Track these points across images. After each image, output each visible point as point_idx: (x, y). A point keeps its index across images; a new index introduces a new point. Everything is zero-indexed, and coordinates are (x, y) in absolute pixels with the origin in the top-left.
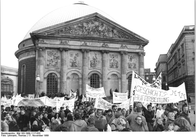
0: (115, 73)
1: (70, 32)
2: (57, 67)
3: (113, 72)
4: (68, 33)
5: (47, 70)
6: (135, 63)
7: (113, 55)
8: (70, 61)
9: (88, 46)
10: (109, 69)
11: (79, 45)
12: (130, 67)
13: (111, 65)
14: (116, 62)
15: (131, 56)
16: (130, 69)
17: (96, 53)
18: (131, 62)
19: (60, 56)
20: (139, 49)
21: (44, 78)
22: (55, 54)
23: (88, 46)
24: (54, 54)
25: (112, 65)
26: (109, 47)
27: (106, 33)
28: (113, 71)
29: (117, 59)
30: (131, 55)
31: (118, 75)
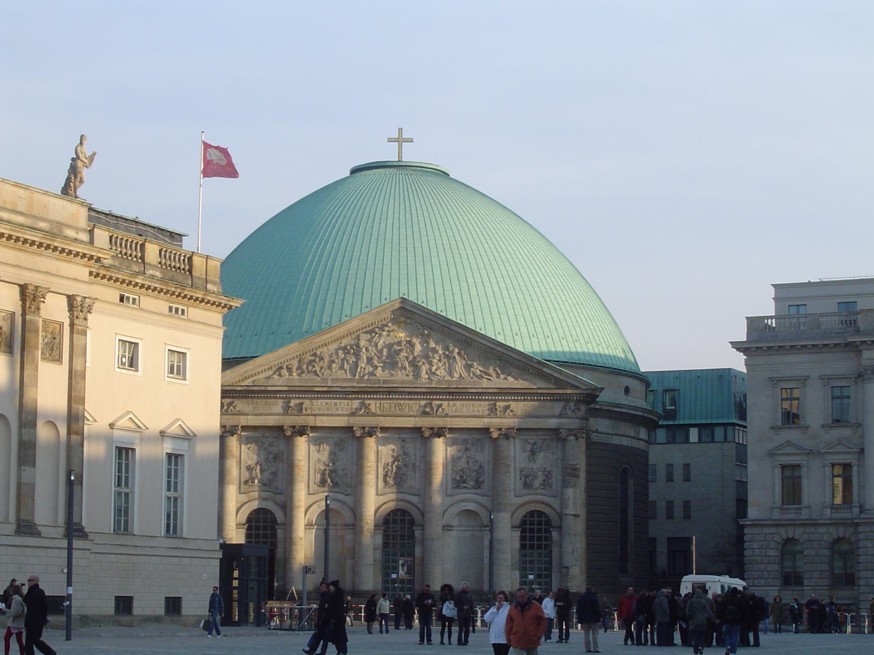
0: (472, 509)
1: (315, 373)
2: (277, 488)
3: (463, 504)
4: (309, 372)
5: (244, 498)
6: (548, 469)
7: (466, 440)
8: (317, 468)
9: (374, 415)
10: (449, 492)
11: (344, 412)
12: (526, 485)
13: (458, 478)
14: (476, 468)
15: (535, 443)
16: (526, 491)
17: (403, 436)
18: (532, 465)
19: (285, 453)
20: (561, 416)
21: (239, 525)
22: (271, 445)
23: (374, 415)
24: (266, 446)
25: (461, 476)
26: (447, 416)
27: (440, 364)
28: (463, 501)
29: (479, 457)
30: (532, 438)
31: (483, 514)
